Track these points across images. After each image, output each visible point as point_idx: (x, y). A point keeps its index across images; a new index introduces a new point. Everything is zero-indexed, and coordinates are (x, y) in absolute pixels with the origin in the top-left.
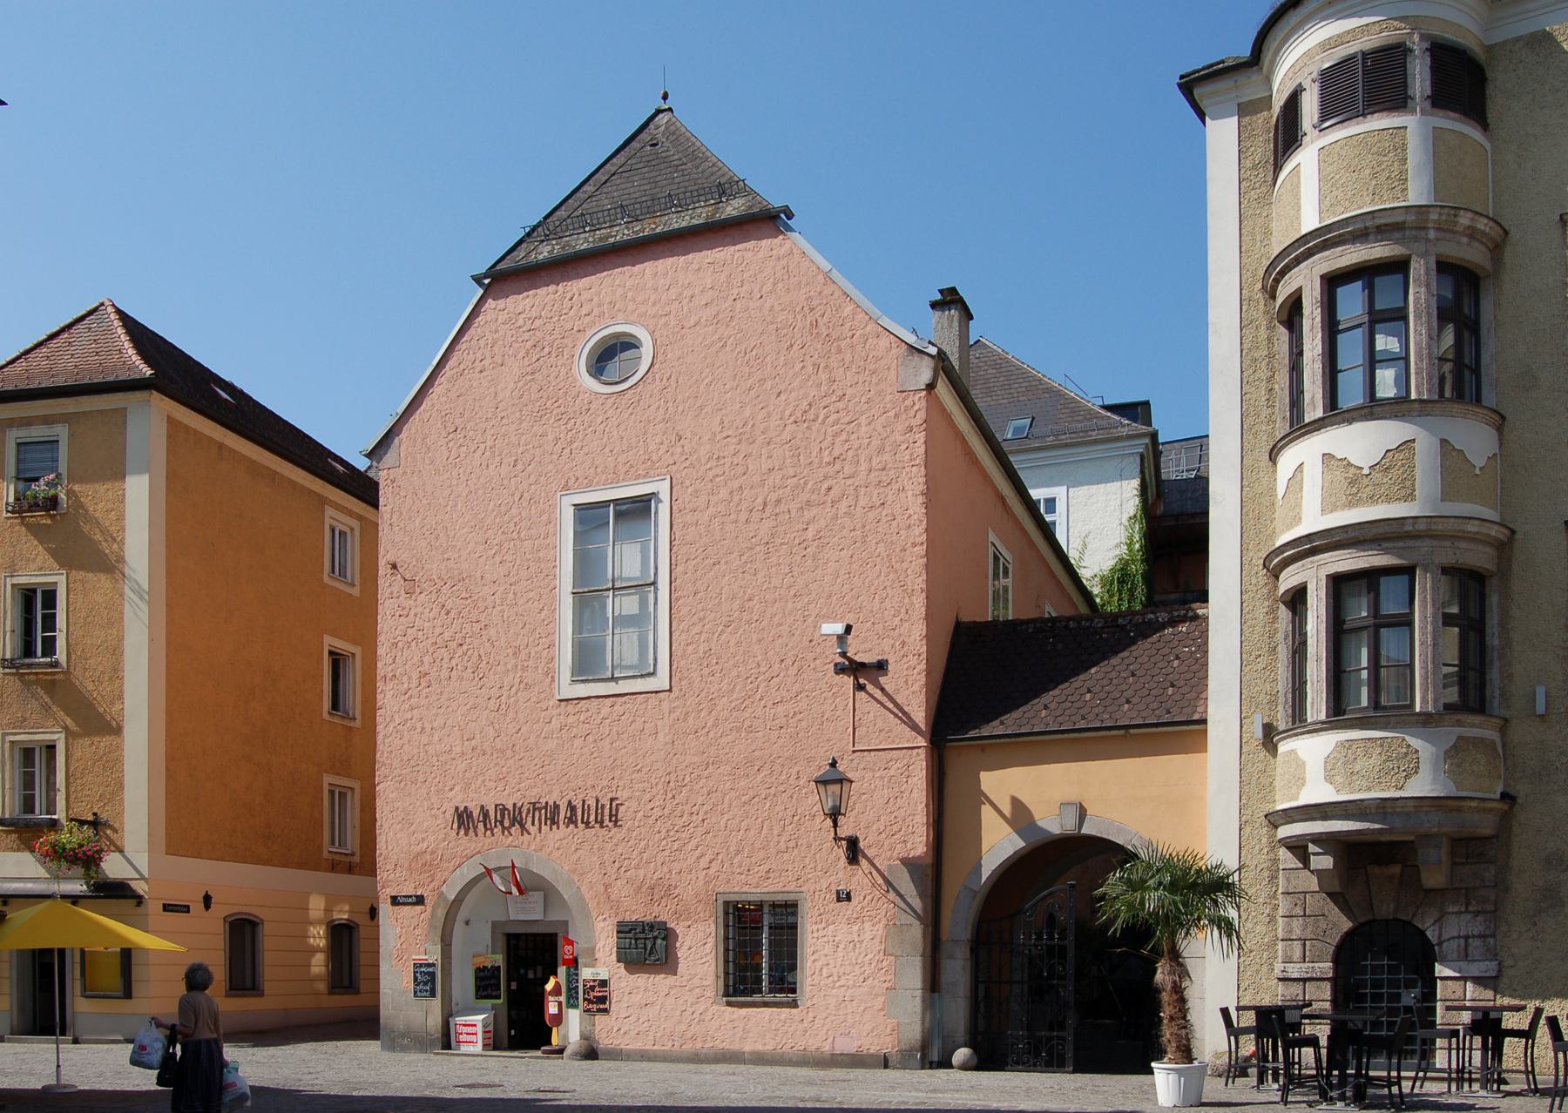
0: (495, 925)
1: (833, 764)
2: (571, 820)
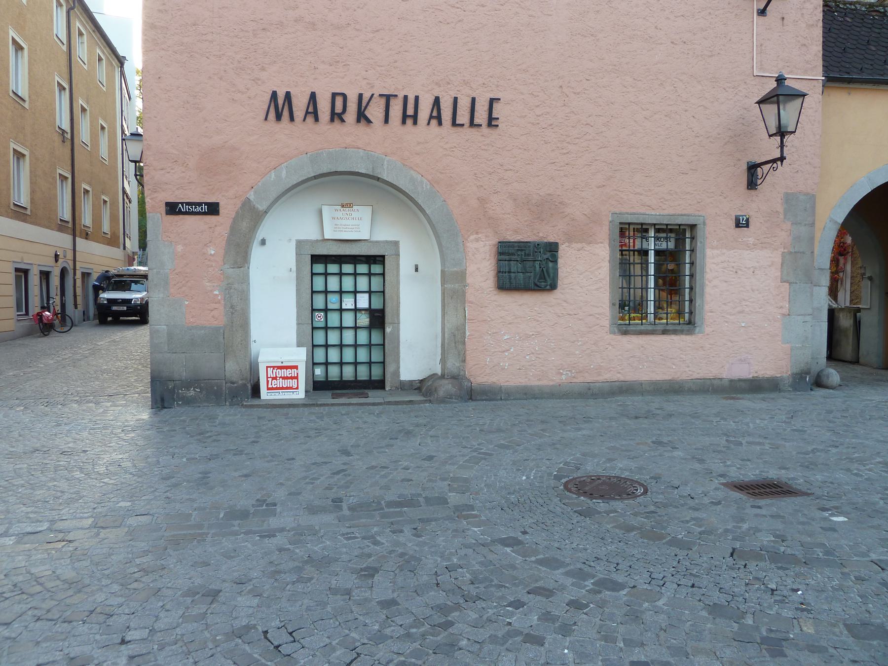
0: (300, 244)
1: (780, 80)
2: (436, 117)
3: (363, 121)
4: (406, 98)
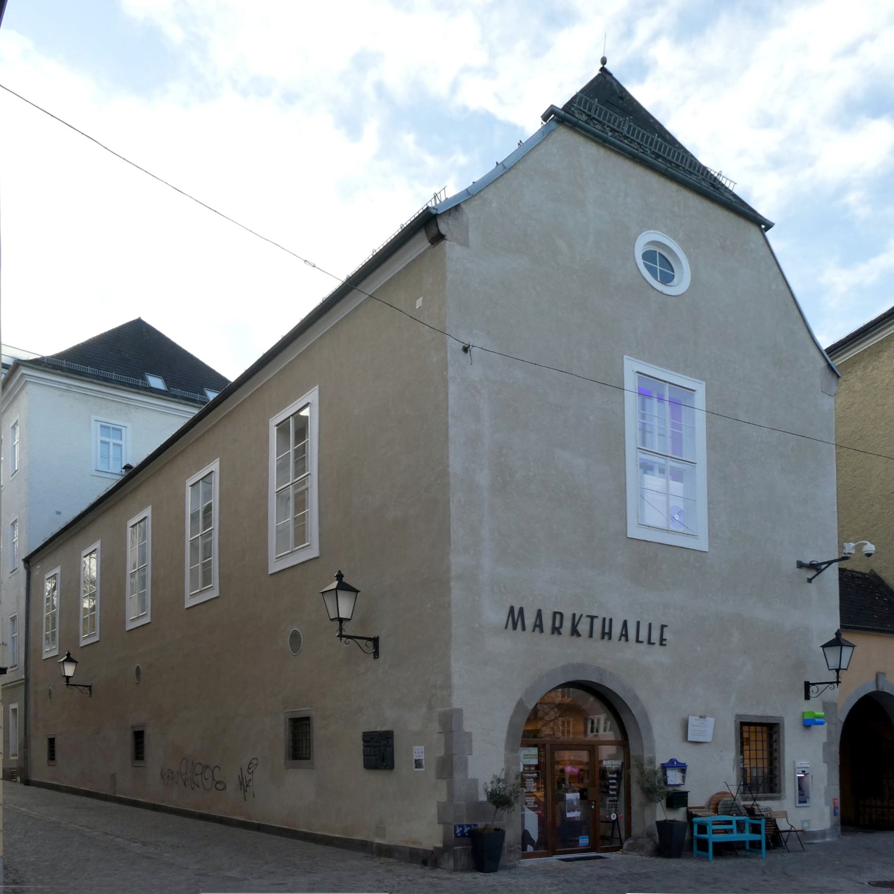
3: (575, 635)
4: (604, 619)
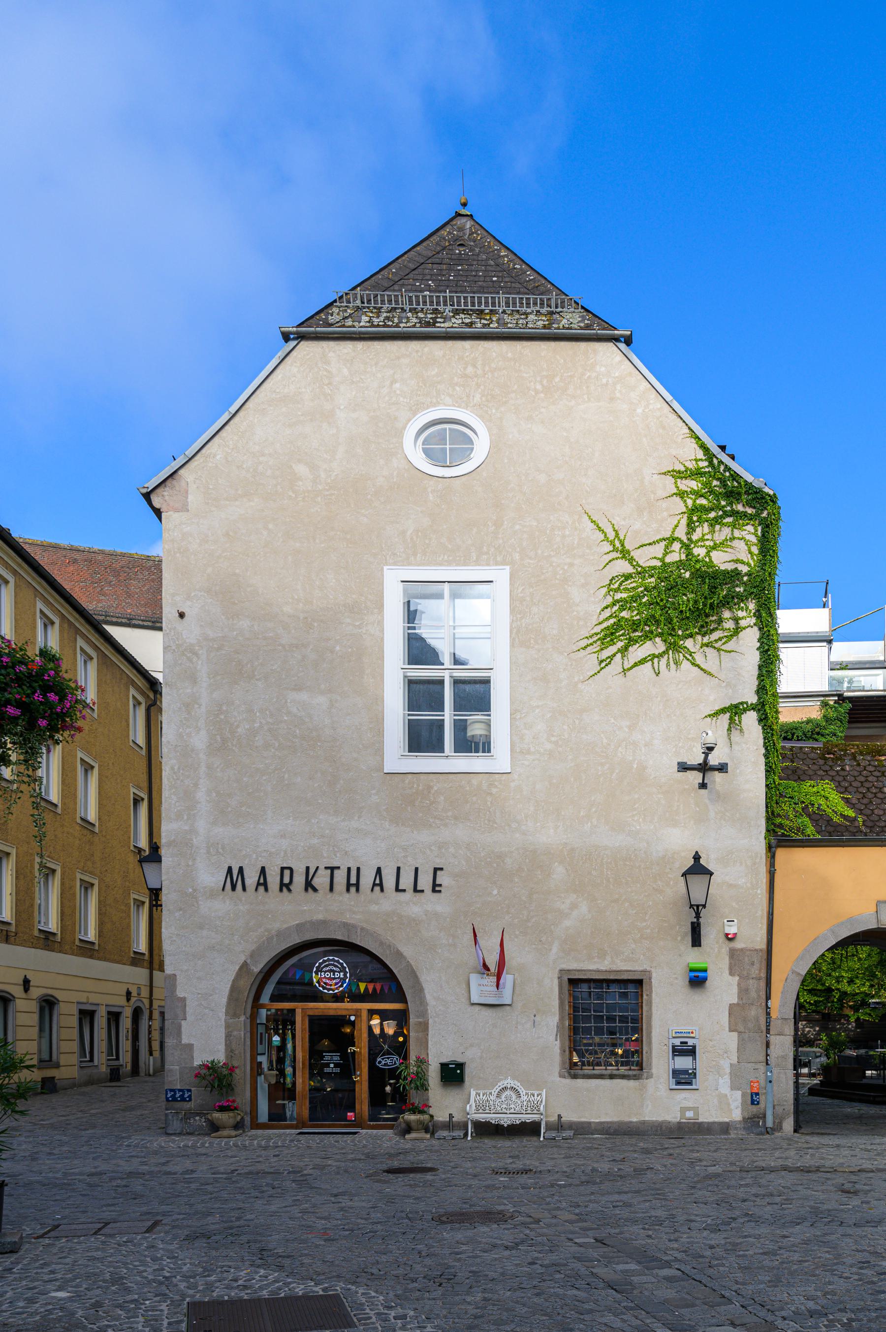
3: (310, 889)
